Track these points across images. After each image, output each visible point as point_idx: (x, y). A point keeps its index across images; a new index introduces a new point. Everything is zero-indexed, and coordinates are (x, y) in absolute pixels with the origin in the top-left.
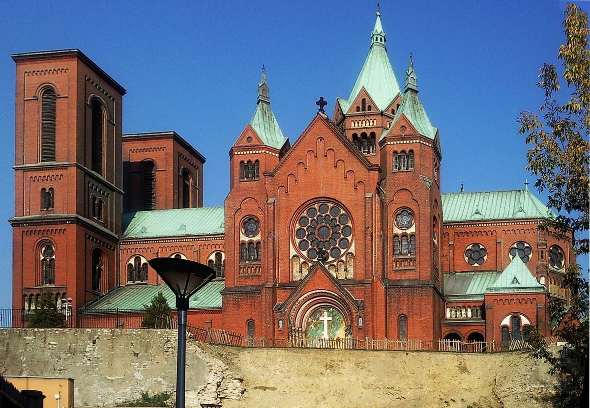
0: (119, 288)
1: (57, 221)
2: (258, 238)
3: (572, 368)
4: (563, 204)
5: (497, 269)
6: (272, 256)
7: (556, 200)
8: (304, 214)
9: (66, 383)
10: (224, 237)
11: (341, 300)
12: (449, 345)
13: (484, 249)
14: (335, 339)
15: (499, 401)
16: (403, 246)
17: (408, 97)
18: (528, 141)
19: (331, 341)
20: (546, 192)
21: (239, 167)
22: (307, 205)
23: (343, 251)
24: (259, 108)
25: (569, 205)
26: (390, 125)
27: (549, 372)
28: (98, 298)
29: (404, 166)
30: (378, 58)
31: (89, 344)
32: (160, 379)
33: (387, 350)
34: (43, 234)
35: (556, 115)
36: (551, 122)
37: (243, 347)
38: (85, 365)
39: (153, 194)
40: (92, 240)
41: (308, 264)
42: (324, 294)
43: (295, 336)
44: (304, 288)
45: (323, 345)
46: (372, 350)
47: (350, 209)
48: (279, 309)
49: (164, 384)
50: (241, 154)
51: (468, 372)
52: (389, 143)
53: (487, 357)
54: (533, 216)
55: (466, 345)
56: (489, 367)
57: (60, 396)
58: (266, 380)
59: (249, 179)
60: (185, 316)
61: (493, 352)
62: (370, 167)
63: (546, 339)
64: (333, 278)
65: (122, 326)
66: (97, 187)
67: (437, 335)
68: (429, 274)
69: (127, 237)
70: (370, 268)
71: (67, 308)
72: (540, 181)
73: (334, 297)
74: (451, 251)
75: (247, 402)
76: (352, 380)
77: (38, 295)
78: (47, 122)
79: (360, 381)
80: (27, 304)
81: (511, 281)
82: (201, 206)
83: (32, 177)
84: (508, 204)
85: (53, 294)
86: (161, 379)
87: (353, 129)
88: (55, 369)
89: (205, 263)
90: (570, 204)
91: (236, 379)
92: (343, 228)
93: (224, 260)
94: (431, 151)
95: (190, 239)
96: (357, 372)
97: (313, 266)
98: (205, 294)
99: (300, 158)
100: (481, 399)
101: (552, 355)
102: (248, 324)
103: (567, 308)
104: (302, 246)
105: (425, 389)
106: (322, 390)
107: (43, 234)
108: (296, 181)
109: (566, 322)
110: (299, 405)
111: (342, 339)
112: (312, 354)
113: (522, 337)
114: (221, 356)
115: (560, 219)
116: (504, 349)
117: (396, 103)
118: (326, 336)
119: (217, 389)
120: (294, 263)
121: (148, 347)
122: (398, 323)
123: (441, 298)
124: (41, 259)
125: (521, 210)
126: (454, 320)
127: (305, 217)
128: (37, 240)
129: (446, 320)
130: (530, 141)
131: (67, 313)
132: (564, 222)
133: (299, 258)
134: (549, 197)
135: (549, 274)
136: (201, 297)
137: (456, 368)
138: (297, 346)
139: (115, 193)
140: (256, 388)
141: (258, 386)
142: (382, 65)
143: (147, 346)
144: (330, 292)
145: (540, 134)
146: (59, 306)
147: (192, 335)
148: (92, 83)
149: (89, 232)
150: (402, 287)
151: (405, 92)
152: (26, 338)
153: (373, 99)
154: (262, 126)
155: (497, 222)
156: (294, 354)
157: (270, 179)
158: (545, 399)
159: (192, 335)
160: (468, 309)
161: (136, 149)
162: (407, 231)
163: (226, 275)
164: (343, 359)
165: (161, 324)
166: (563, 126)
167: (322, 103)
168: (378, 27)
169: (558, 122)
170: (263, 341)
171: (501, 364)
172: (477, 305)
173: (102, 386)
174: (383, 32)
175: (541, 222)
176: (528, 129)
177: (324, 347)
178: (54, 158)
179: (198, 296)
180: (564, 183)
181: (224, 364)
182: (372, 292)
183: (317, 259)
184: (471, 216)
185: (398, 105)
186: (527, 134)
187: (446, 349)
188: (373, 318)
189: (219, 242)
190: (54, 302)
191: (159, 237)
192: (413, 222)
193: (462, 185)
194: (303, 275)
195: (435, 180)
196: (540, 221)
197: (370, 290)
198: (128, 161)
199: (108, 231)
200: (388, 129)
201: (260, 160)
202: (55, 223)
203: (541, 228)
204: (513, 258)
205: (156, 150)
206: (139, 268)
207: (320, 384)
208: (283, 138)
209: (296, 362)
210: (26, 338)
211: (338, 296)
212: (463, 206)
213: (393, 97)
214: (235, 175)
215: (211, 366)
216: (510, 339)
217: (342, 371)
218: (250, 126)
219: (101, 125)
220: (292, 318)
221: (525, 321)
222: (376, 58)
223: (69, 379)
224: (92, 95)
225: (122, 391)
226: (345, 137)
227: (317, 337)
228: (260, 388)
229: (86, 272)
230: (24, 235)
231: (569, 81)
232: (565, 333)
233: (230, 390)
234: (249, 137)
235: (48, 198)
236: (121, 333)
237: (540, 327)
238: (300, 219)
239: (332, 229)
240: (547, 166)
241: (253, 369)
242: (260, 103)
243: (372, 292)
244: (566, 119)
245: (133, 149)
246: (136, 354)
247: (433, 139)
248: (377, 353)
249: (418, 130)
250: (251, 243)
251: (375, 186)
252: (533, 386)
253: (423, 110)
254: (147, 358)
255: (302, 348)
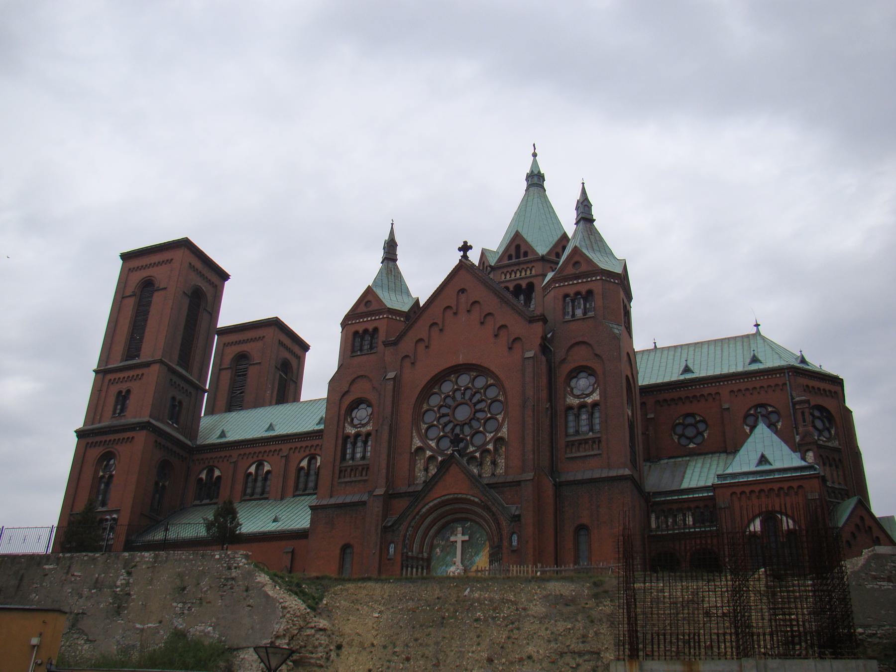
120: (417, 458)
162: (586, 399)
183: (452, 450)
192: (596, 385)
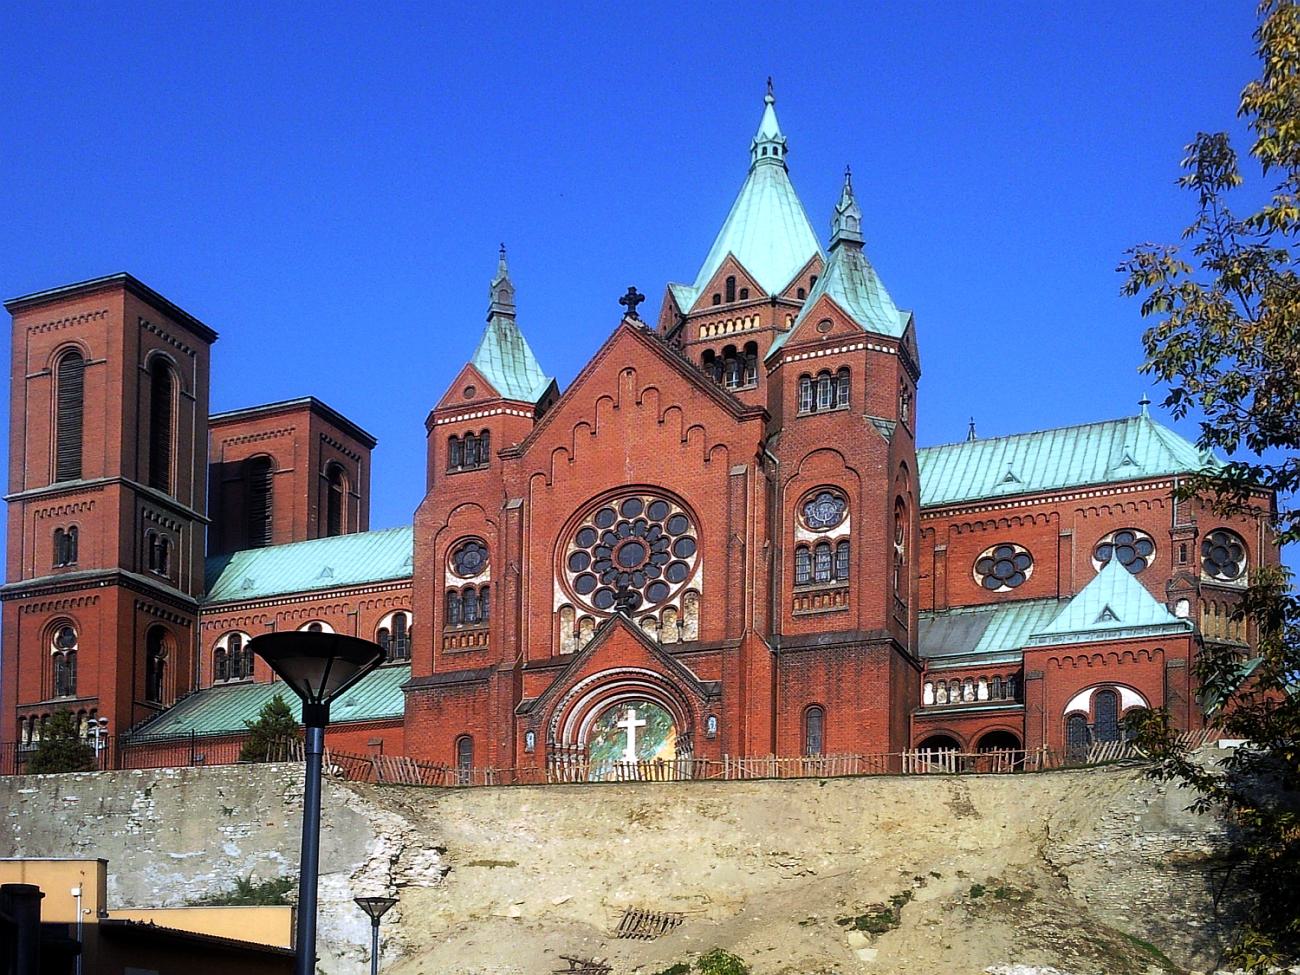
0: (196, 693)
1: (83, 584)
2: (484, 578)
3: (1260, 795)
4: (1244, 437)
5: (1060, 594)
6: (514, 611)
7: (1224, 431)
8: (588, 523)
9: (92, 869)
10: (411, 583)
11: (667, 684)
12: (929, 760)
13: (1028, 556)
14: (652, 763)
15: (1056, 874)
16: (819, 567)
17: (840, 257)
18: (1147, 309)
19: (643, 767)
20: (1196, 415)
21: (445, 447)
22: (596, 505)
23: (674, 588)
24: (491, 329)
25: (1259, 437)
26: (792, 321)
27: (1193, 809)
28: (157, 714)
29: (825, 402)
30: (768, 189)
31: (138, 797)
32: (273, 854)
33: (775, 778)
34: (56, 608)
35: (1227, 242)
36: (1213, 258)
37: (448, 788)
38: (130, 834)
39: (268, 517)
40: (148, 611)
41: (593, 620)
42: (628, 676)
43: (562, 762)
44: (584, 666)
45: (623, 776)
46: (738, 780)
47: (694, 502)
48: (526, 712)
49: (282, 863)
50: (450, 422)
51: (976, 815)
52: (789, 359)
53: (1025, 782)
54: (1161, 471)
55: (973, 759)
56: (1032, 800)
57: (81, 891)
58: (495, 847)
59: (466, 469)
60: (321, 738)
61: (1042, 770)
62: (742, 415)
63: (1187, 737)
64: (651, 643)
65: (203, 762)
66: (158, 516)
67: (899, 739)
68: (882, 617)
69: (215, 600)
70: (738, 616)
71: (97, 735)
72: (1177, 394)
73: (652, 679)
74: (938, 565)
75: (453, 890)
76: (689, 840)
77: (45, 716)
78: (68, 412)
79: (708, 844)
80: (24, 734)
81: (1096, 616)
82: (365, 528)
83: (38, 511)
84: (1092, 451)
85: (73, 713)
86: (276, 854)
87: (705, 341)
88: (73, 844)
89: (372, 638)
90: (1262, 434)
91: (431, 848)
92: (677, 542)
93: (411, 627)
94: (895, 363)
95: (341, 592)
96: (702, 825)
97: (605, 622)
98: (369, 694)
99: (581, 414)
100: (1008, 870)
101: (1202, 770)
102: (459, 744)
103: (1248, 667)
104: (582, 584)
105: (866, 852)
106: (619, 863)
107: (56, 608)
108: (569, 460)
109: (1242, 697)
110: (568, 893)
111: (669, 761)
112: (599, 794)
113: (1123, 734)
114: (401, 806)
115: (1233, 471)
116: (1072, 760)
117: (810, 275)
118: (630, 755)
119: (390, 869)
120: (562, 619)
121: (250, 797)
122: (802, 721)
123: (911, 665)
124: (52, 653)
125: (1129, 461)
126: (943, 708)
127: (588, 528)
128: (45, 621)
129: (923, 709)
130: (1155, 308)
131: (98, 745)
132: (1246, 476)
133: (574, 610)
134: (1203, 424)
135: (1200, 594)
136: (361, 700)
137: (946, 807)
138: (565, 780)
139: (194, 524)
140: (472, 864)
141: (478, 859)
142: (776, 201)
143: (251, 794)
144: (644, 671)
145: (1181, 290)
146: (83, 733)
147: (341, 769)
148: (152, 330)
149: (141, 598)
150: (815, 649)
151: (832, 249)
152: (22, 791)
153: (753, 275)
154: (497, 364)
155: (1060, 494)
156: (559, 796)
157: (513, 463)
158: (1182, 866)
159: (341, 769)
160: (980, 683)
161: (235, 438)
162: (829, 534)
163: (414, 655)
164: (669, 801)
165: (278, 754)
166: (1249, 263)
167: (632, 299)
168: (770, 125)
169: (1234, 257)
170: (491, 775)
171: (1064, 793)
172: (1003, 672)
173: (160, 870)
174: (779, 134)
175: (1182, 483)
176: (1148, 282)
177: (626, 779)
178: (80, 473)
179: (356, 698)
180: (1247, 390)
181: (405, 822)
182: (742, 663)
184: (994, 487)
185: (814, 279)
186: (1145, 294)
187: (921, 769)
188: (741, 718)
189: (401, 593)
190: (74, 727)
191: (279, 595)
192: (845, 513)
193: (972, 424)
194: (583, 642)
195: (903, 423)
196: (1179, 481)
197: (735, 661)
198: (220, 461)
199: (178, 593)
200: (788, 331)
201: (490, 427)
202: (79, 587)
203: (1181, 494)
204: (1102, 567)
205: (276, 436)
206: (237, 655)
207: (615, 853)
208: (542, 379)
209: (562, 811)
210: (22, 791)
211: (661, 677)
212: (972, 468)
213: (802, 263)
214: (438, 463)
215: (379, 826)
216: (1089, 741)
217: (666, 823)
218: (472, 366)
219: (168, 403)
220: (554, 727)
221: (1130, 699)
222: (762, 190)
223: (99, 860)
224: (150, 352)
225: (198, 878)
226: (684, 360)
227: (610, 760)
228: (483, 863)
229: (134, 669)
230: (23, 613)
231: (1268, 161)
232: (1241, 720)
233: (418, 869)
234: (469, 388)
235: (66, 546)
236: (200, 774)
237: (1171, 711)
238: (579, 533)
239: (651, 545)
240: (1200, 359)
241: (466, 827)
242: (495, 318)
243: (742, 663)
244: (1257, 247)
245: (229, 439)
246: (227, 811)
247: (900, 336)
248: (751, 785)
249: (861, 323)
250: (468, 588)
251: (755, 449)
252: (1150, 839)
253: (877, 279)
254: (248, 816)
255: (577, 783)
